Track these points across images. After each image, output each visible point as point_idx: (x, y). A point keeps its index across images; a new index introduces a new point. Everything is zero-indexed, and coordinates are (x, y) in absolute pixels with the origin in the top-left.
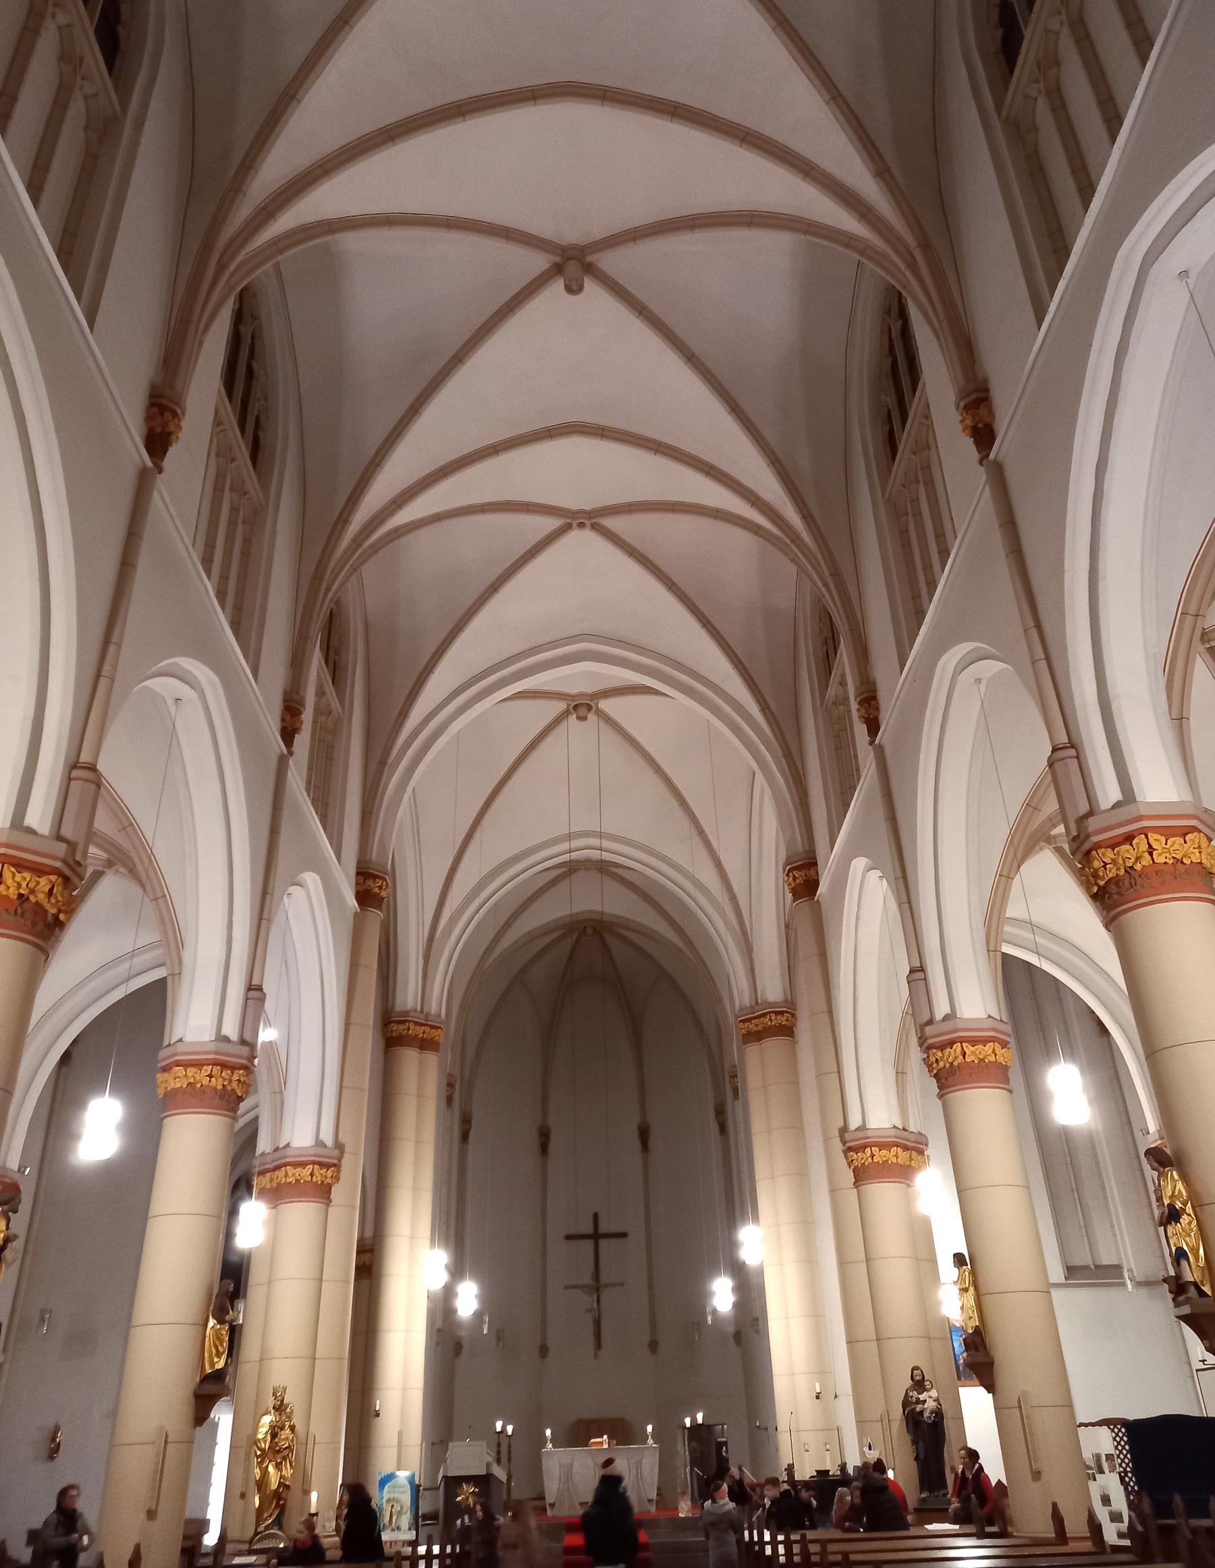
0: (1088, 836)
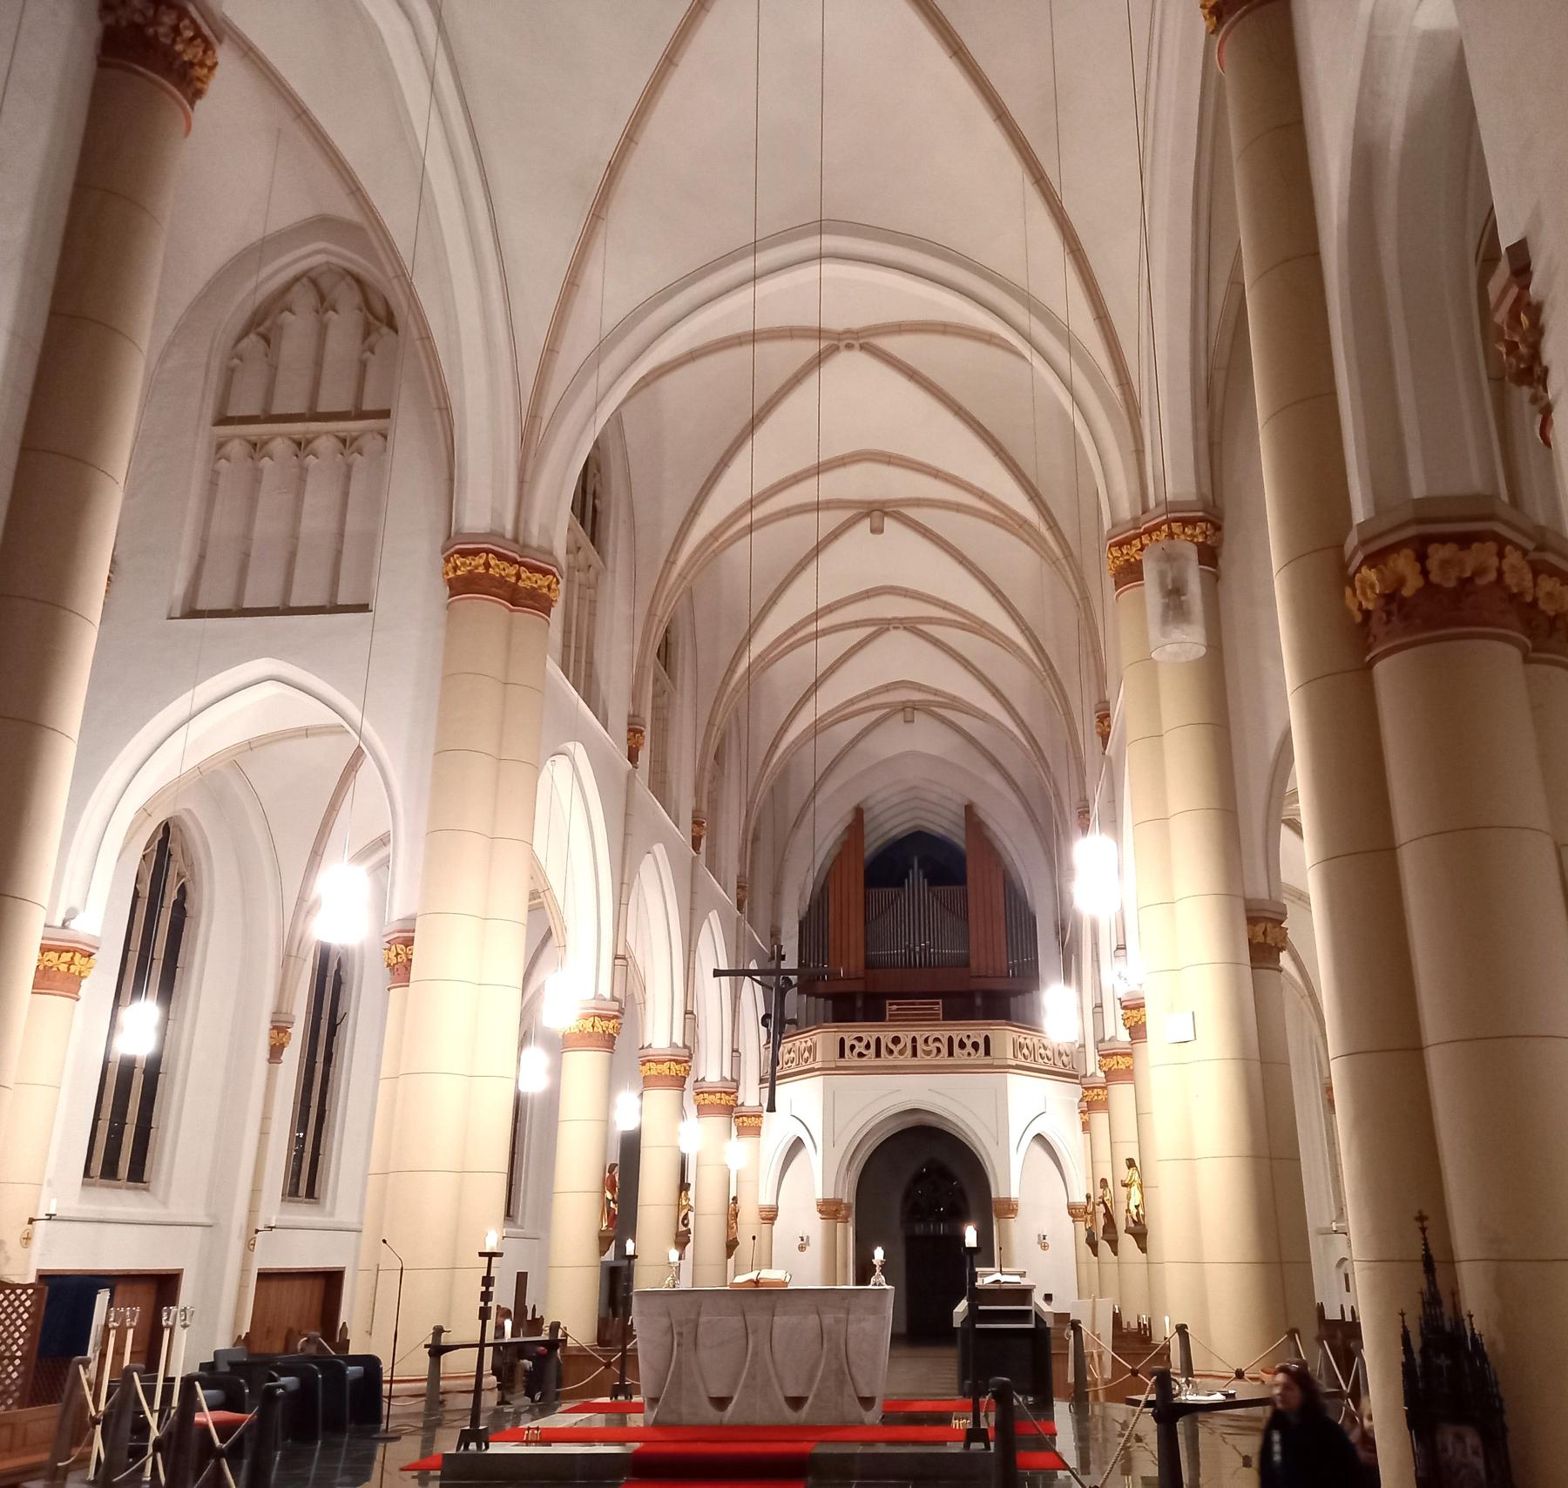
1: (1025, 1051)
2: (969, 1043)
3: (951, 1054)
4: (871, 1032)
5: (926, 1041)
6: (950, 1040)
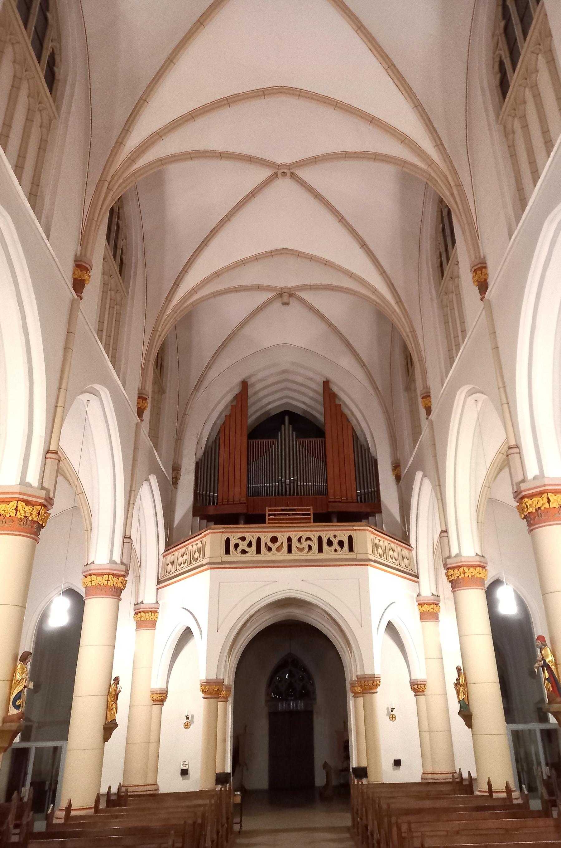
0: (521, 492)
1: (380, 551)
2: (335, 542)
3: (320, 550)
4: (252, 533)
5: (299, 540)
6: (320, 539)
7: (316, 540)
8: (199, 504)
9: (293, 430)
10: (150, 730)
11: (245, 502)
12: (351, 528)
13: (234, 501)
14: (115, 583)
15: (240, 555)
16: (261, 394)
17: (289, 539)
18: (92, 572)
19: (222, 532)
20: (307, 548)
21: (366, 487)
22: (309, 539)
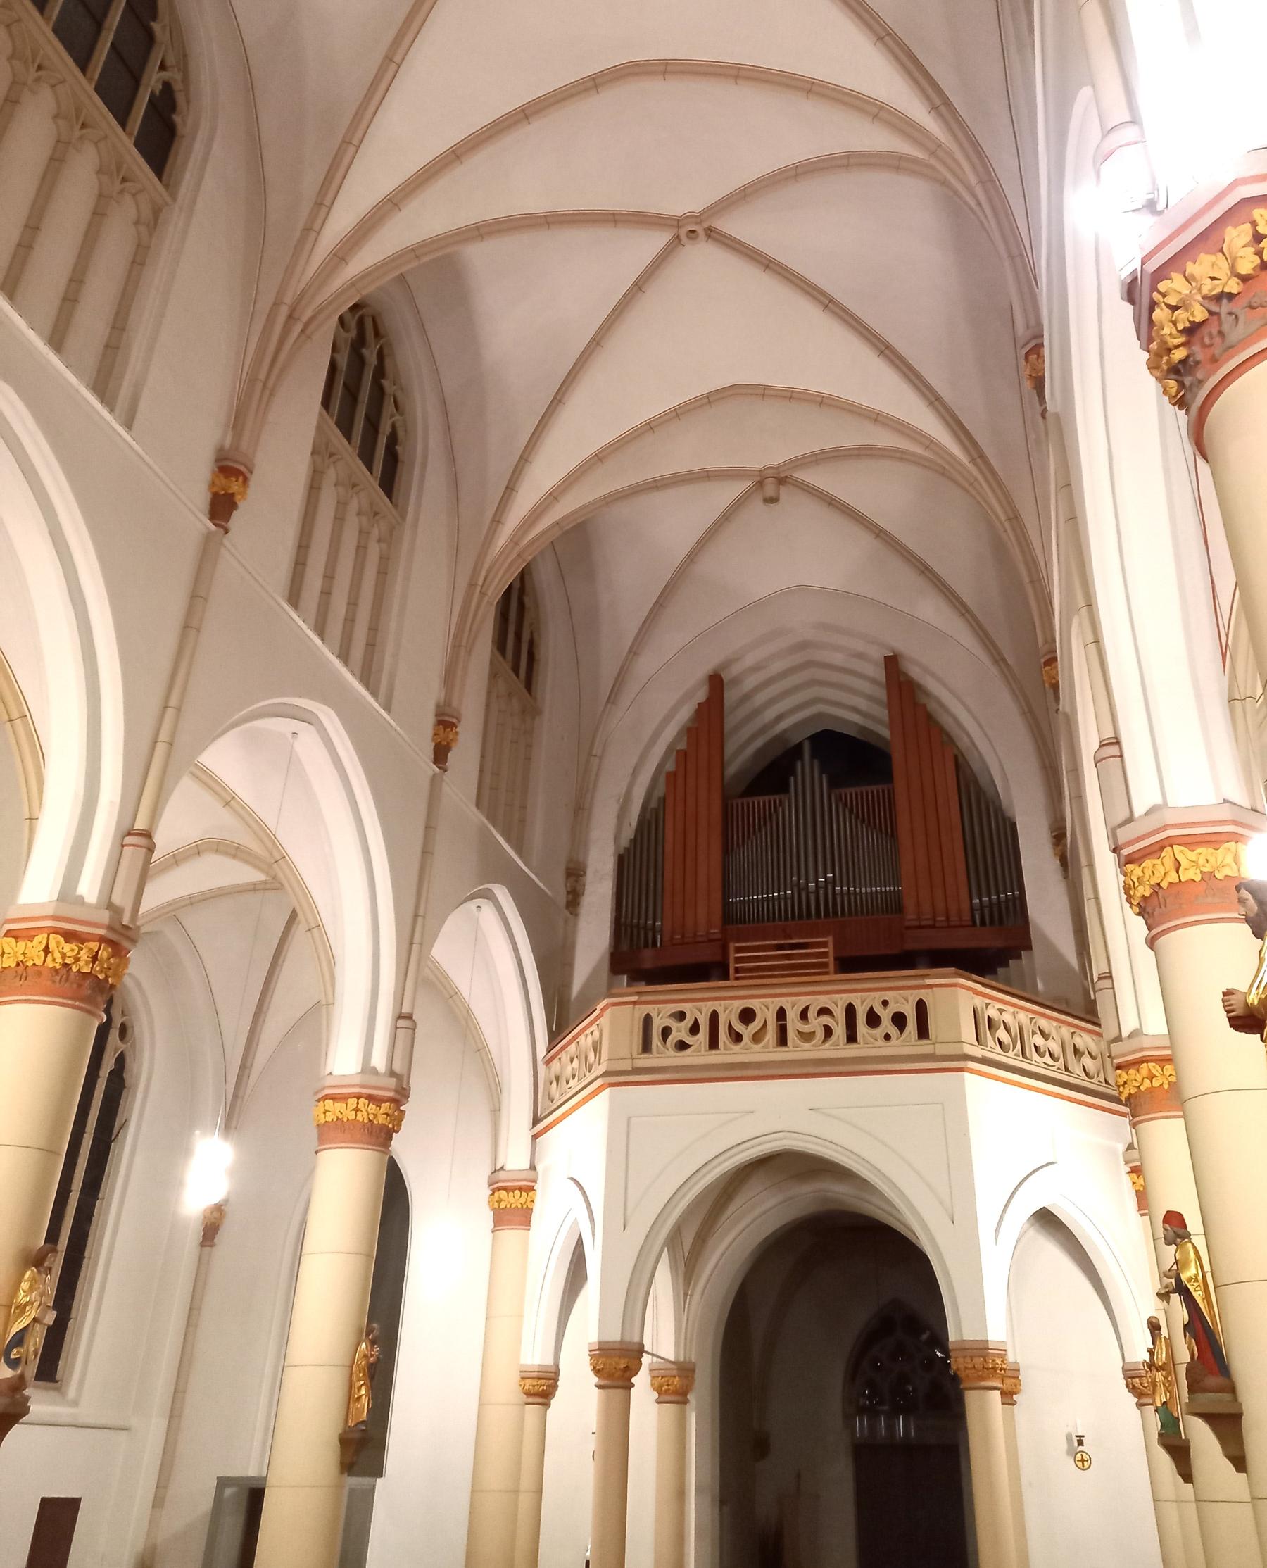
1: (1002, 1034)
2: (886, 1015)
3: (852, 1038)
4: (699, 1002)
5: (804, 1015)
6: (850, 1011)
7: (840, 1013)
8: (625, 947)
9: (821, 773)
10: (518, 1463)
11: (719, 936)
12: (920, 982)
13: (695, 935)
14: (371, 1117)
15: (672, 1052)
16: (760, 699)
17: (781, 1014)
18: (327, 1092)
19: (634, 1003)
20: (820, 1034)
21: (993, 891)
22: (824, 1011)
